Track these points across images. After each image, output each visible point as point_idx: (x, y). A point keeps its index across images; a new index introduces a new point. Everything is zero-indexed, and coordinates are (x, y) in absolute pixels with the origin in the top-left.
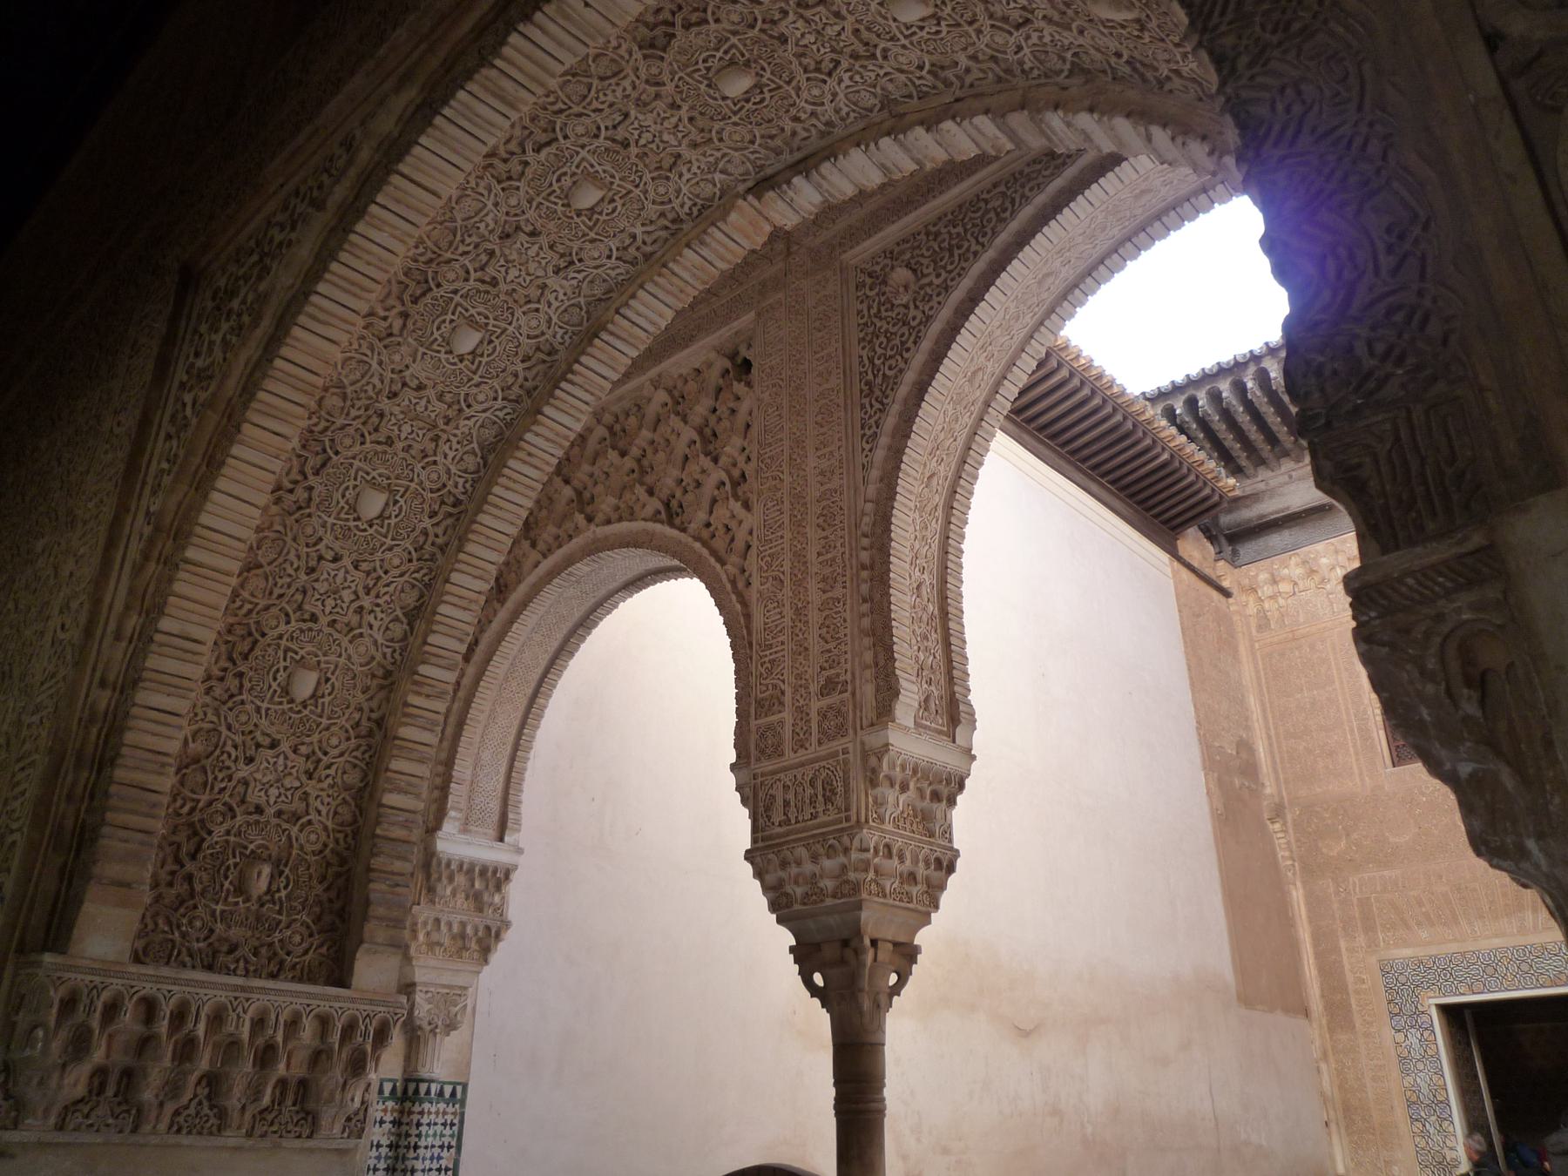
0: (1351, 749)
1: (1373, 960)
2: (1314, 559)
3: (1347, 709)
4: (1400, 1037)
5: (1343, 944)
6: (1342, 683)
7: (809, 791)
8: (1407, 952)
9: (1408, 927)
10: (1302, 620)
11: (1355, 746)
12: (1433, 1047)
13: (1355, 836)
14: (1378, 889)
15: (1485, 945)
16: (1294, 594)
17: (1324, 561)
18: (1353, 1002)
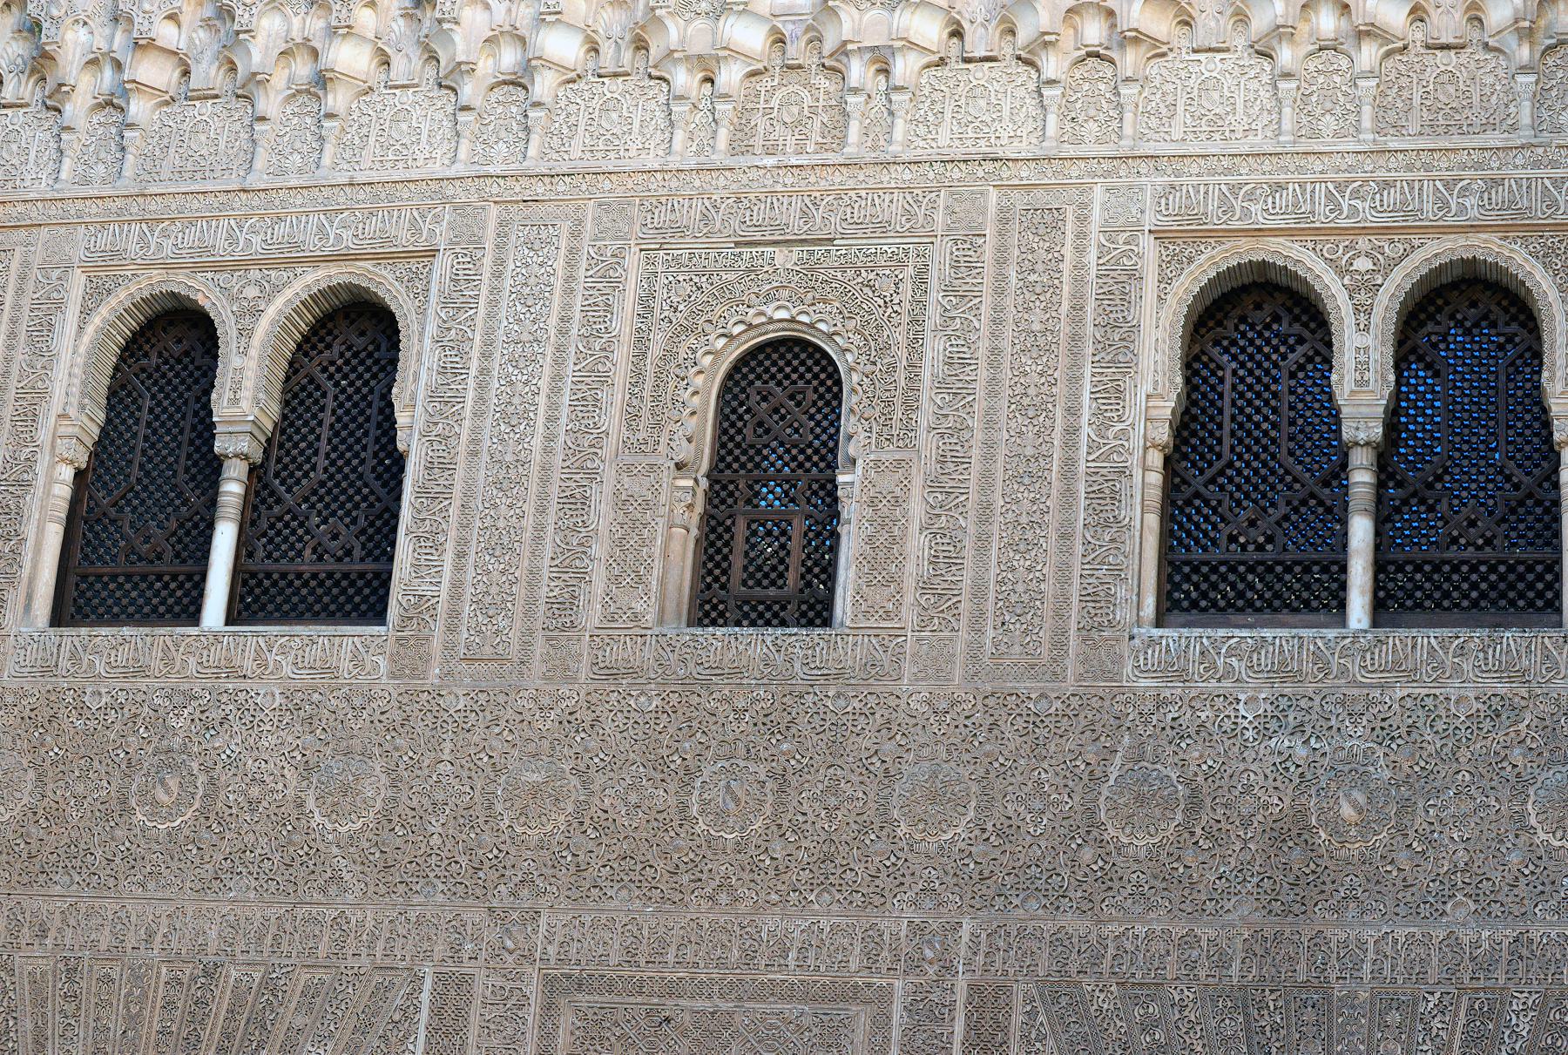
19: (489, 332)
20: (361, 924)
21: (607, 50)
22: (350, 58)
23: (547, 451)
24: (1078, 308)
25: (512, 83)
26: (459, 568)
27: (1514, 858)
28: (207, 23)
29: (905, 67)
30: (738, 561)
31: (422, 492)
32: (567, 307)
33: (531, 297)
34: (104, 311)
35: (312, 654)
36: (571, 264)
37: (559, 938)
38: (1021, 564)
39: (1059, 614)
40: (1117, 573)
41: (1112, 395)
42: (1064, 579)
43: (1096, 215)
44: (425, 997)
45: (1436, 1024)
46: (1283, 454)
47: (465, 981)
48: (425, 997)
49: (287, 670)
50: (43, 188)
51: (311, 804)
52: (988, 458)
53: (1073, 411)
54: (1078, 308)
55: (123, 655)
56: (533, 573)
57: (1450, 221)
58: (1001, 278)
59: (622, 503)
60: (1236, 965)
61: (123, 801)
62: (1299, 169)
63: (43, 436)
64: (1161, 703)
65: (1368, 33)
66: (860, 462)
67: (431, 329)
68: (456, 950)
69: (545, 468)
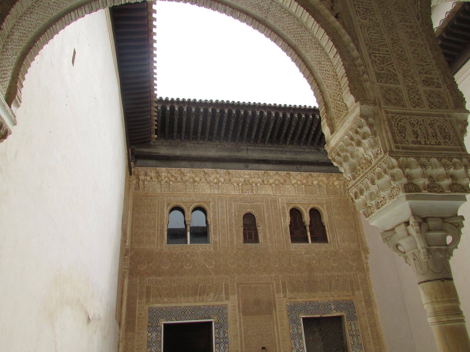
0: (156, 236)
1: (146, 307)
2: (161, 172)
3: (158, 223)
4: (150, 334)
5: (138, 301)
6: (158, 214)
7: (430, 130)
8: (159, 305)
9: (160, 296)
10: (150, 190)
11: (157, 235)
12: (160, 338)
13: (150, 264)
14: (154, 283)
15: (183, 305)
16: (150, 181)
17: (163, 174)
18: (136, 321)
19: (218, 211)
20: (215, 278)
21: (226, 180)
22: (197, 179)
23: (227, 225)
24: (280, 211)
25: (216, 183)
26: (219, 238)
27: (330, 266)
28: (179, 174)
29: (258, 185)
30: (247, 236)
31: (213, 229)
32: (226, 209)
33: (222, 207)
34: (170, 207)
35: (204, 247)
36: (226, 204)
37: (237, 279)
38: (279, 237)
39: (283, 242)
40: (288, 238)
41: (285, 220)
42: (283, 239)
43: (280, 201)
44: (224, 286)
45: (326, 283)
46: (298, 226)
47: (228, 284)
48: (224, 286)
49: (201, 249)
50: (159, 191)
51: (206, 265)
52: (274, 226)
53: (281, 221)
54: (280, 211)
55: (180, 248)
56: (228, 238)
57: (313, 203)
58: (271, 207)
59: (236, 230)
60: (307, 279)
61: (183, 265)
62: (299, 197)
63: (165, 221)
64: (295, 251)
65: (304, 184)
66: (261, 226)
67: (211, 211)
68: (226, 281)
69: (227, 226)
